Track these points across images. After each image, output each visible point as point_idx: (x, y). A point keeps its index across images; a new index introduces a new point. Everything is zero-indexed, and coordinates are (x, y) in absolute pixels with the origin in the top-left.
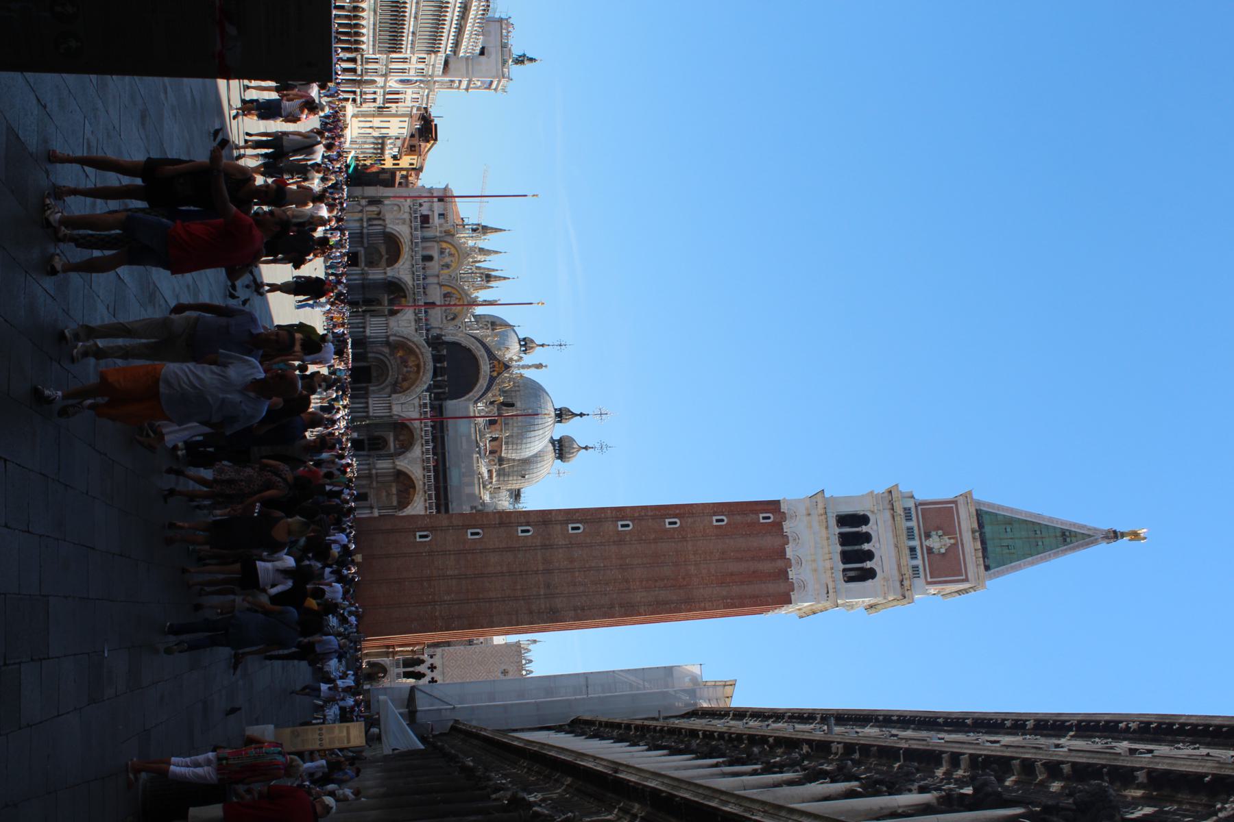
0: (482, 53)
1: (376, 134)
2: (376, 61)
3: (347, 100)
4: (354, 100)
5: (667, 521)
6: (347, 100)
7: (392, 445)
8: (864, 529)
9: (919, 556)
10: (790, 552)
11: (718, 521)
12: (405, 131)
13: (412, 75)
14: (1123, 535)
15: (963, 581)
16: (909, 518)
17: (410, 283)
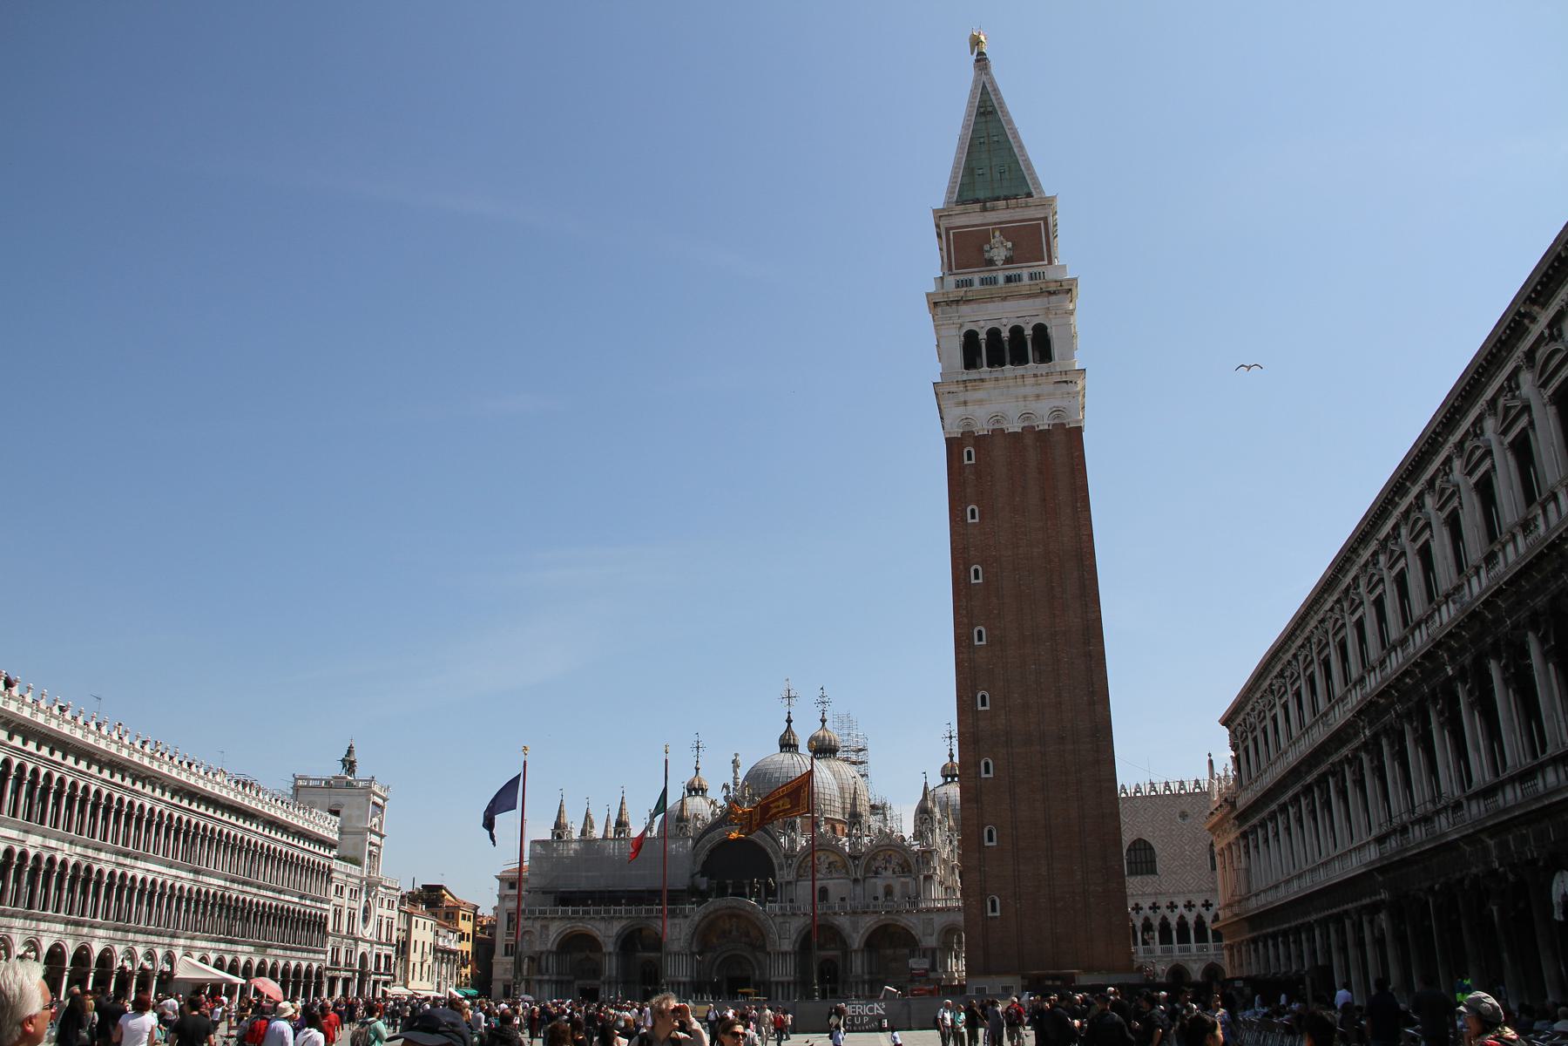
0: (336, 813)
1: (430, 959)
2: (336, 951)
3: (384, 993)
4: (386, 984)
5: (973, 581)
6: (384, 993)
7: (831, 953)
8: (983, 336)
9: (1018, 272)
10: (1015, 427)
11: (973, 517)
12: (429, 923)
13: (359, 905)
14: (981, 54)
15: (1046, 224)
16: (970, 283)
17: (624, 923)
